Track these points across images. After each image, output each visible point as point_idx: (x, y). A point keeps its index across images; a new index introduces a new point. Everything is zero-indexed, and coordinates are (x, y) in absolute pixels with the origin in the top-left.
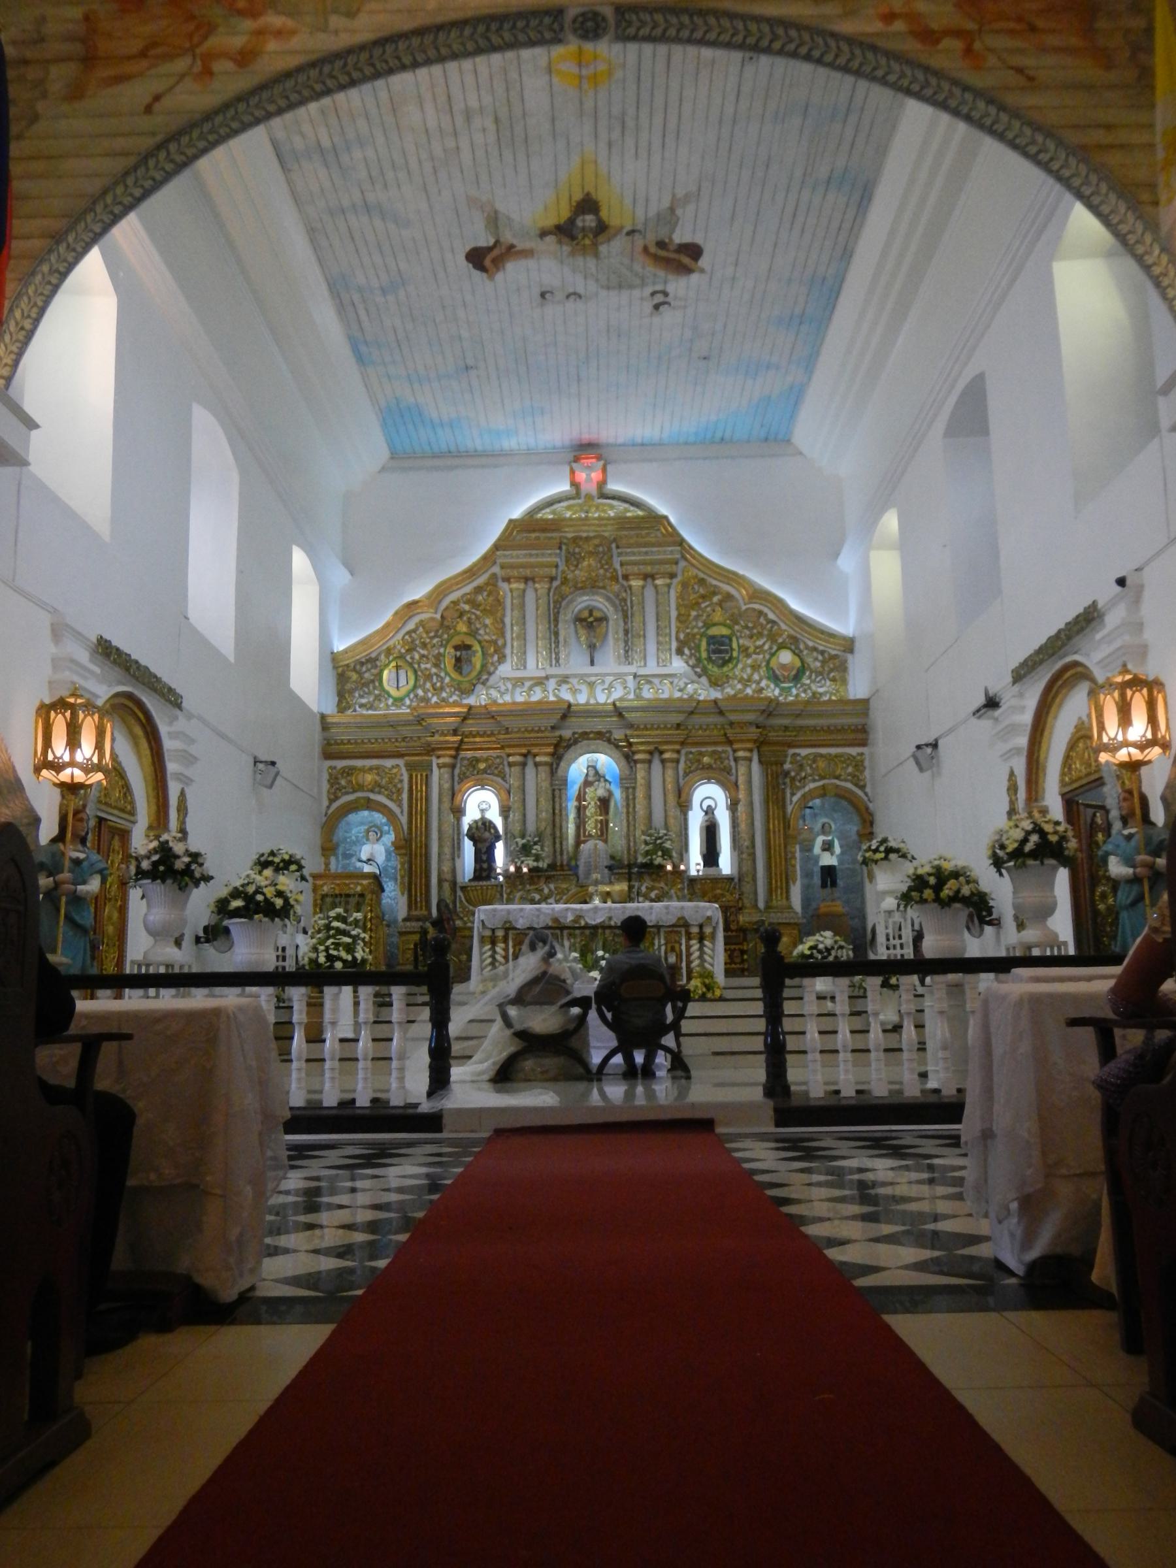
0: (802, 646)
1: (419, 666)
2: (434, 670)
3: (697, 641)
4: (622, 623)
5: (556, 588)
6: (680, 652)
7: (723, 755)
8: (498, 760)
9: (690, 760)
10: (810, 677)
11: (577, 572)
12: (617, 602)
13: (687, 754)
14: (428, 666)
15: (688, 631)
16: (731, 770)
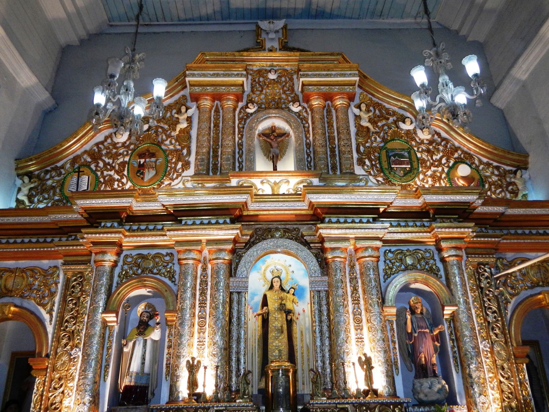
0: (477, 162)
1: (102, 173)
2: (116, 177)
3: (376, 154)
4: (305, 139)
5: (242, 108)
6: (361, 162)
7: (428, 255)
8: (167, 258)
9: (390, 261)
10: (490, 189)
11: (262, 96)
12: (300, 121)
13: (385, 252)
14: (112, 173)
15: (367, 145)
16: (439, 270)
